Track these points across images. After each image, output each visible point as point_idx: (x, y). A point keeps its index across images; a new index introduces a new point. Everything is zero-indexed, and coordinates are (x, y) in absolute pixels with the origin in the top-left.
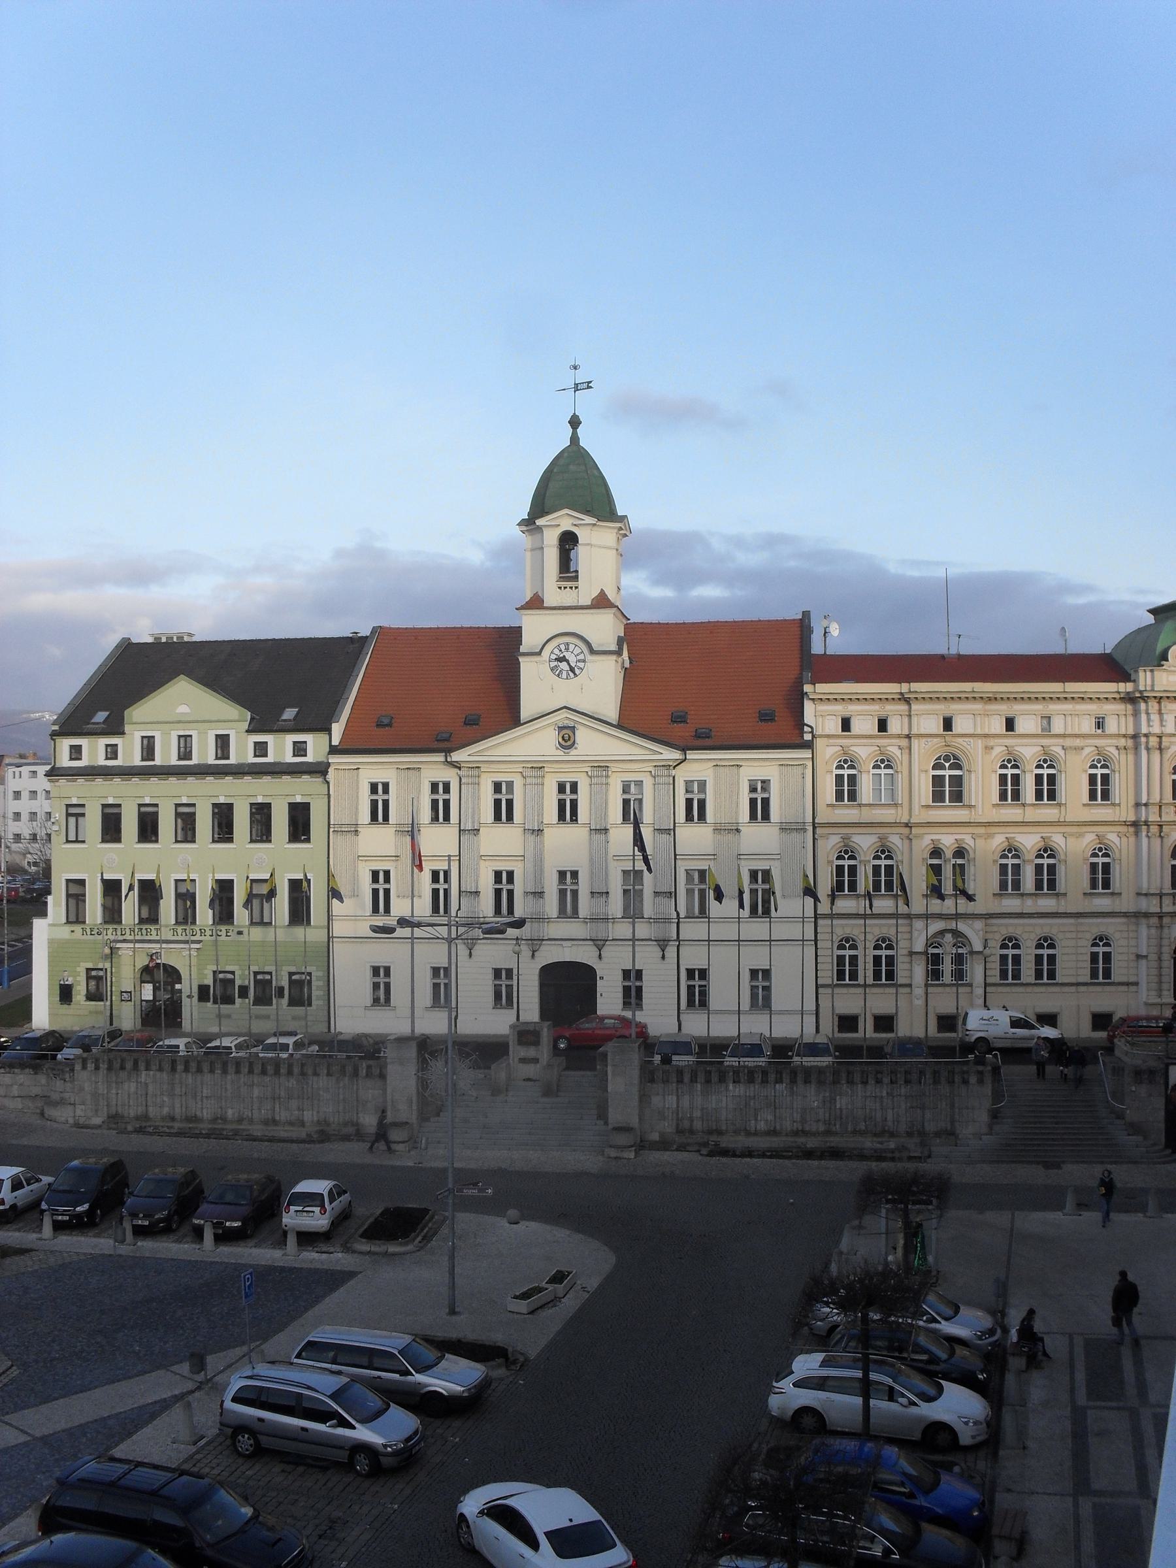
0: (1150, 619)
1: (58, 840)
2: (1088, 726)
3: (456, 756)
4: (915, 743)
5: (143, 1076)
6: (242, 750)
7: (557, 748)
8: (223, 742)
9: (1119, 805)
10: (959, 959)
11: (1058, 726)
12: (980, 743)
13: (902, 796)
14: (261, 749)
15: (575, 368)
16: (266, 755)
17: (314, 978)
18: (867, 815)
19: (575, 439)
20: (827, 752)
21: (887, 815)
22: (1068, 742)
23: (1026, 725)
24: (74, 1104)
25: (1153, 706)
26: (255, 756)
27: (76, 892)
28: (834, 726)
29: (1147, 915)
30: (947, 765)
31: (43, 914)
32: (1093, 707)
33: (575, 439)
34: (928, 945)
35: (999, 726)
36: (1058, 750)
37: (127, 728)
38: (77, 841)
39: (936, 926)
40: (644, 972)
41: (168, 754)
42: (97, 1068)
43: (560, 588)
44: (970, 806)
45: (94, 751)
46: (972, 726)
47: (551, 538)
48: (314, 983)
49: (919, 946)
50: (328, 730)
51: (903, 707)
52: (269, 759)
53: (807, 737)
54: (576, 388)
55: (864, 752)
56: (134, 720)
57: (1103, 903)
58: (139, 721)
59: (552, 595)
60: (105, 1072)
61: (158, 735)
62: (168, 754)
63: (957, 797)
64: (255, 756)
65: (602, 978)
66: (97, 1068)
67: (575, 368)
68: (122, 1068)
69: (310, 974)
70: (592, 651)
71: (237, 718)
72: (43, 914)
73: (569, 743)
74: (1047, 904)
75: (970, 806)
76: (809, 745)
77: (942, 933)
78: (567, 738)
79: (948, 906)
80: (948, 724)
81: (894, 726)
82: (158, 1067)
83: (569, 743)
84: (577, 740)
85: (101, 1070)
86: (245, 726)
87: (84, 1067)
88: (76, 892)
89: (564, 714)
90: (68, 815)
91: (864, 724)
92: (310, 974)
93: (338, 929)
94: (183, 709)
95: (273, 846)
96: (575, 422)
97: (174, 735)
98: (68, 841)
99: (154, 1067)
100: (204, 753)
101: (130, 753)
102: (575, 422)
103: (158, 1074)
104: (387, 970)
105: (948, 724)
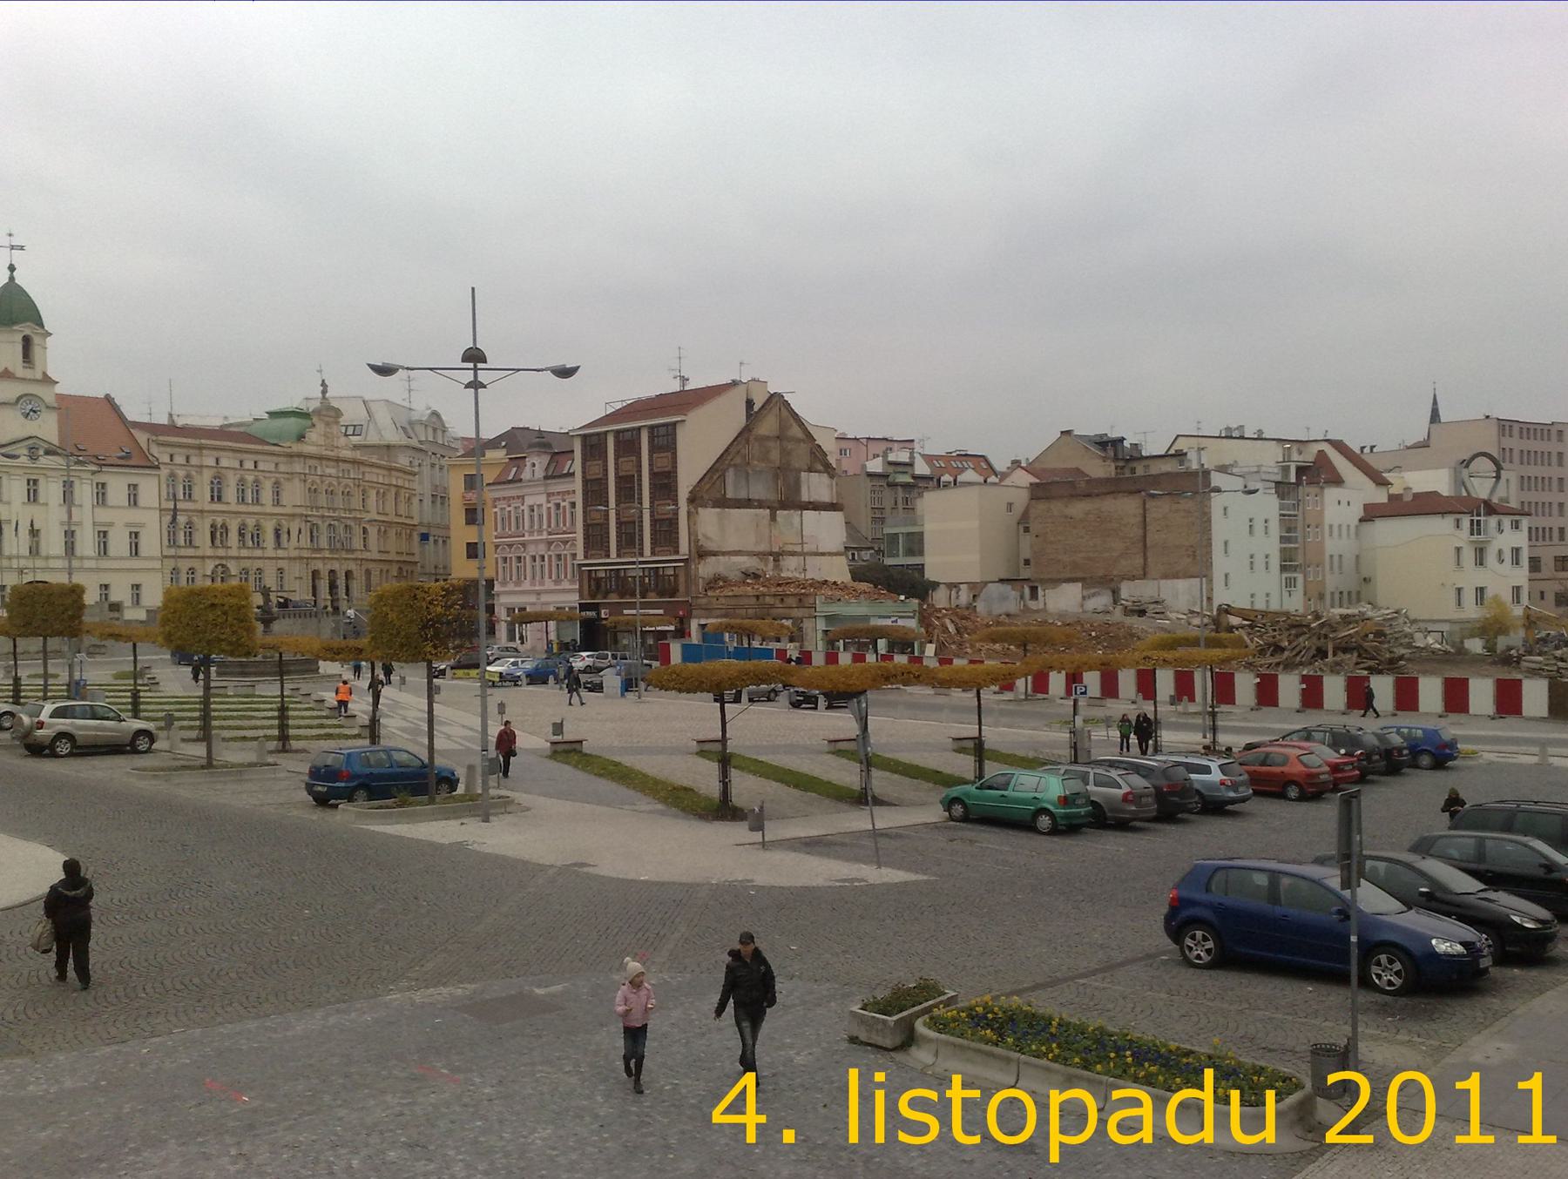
0: (266, 416)
2: (272, 467)
11: (261, 466)
12: (232, 471)
15: (10, 235)
19: (12, 279)
20: (164, 472)
22: (267, 475)
25: (302, 459)
28: (167, 460)
29: (301, 558)
32: (275, 459)
33: (12, 279)
39: (217, 563)
47: (19, 338)
51: (197, 452)
54: (12, 247)
55: (181, 473)
63: (219, 498)
67: (10, 235)
70: (48, 407)
74: (258, 553)
75: (228, 503)
76: (157, 468)
77: (216, 567)
79: (221, 552)
81: (194, 461)
89: (30, 442)
91: (180, 460)
96: (12, 268)
102: (12, 268)
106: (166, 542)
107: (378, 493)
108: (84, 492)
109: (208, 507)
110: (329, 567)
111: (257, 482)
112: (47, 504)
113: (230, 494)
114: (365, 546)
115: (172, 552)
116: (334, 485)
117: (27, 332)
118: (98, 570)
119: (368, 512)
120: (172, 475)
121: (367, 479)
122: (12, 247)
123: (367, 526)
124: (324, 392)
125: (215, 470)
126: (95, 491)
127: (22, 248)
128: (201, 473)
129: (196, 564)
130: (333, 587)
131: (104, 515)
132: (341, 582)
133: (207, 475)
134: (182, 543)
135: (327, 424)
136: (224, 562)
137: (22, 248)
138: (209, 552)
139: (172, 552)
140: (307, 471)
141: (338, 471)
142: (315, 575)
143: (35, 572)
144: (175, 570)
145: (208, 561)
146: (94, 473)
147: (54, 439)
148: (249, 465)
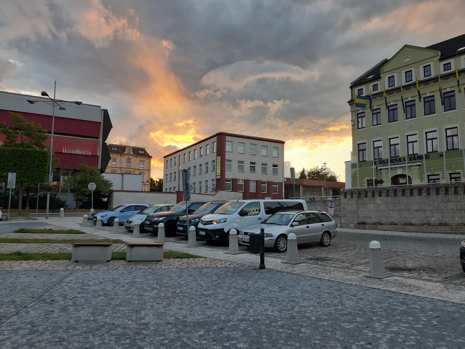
5: (378, 200)
8: (427, 68)
24: (341, 217)
37: (381, 75)
38: (362, 128)
42: (352, 197)
56: (385, 71)
58: (386, 71)
60: (356, 199)
62: (400, 81)
66: (352, 197)
68: (366, 196)
71: (433, 56)
82: (386, 194)
85: (354, 197)
86: (439, 57)
87: (346, 197)
90: (358, 118)
94: (407, 60)
95: (457, 111)
99: (383, 195)
103: (386, 198)
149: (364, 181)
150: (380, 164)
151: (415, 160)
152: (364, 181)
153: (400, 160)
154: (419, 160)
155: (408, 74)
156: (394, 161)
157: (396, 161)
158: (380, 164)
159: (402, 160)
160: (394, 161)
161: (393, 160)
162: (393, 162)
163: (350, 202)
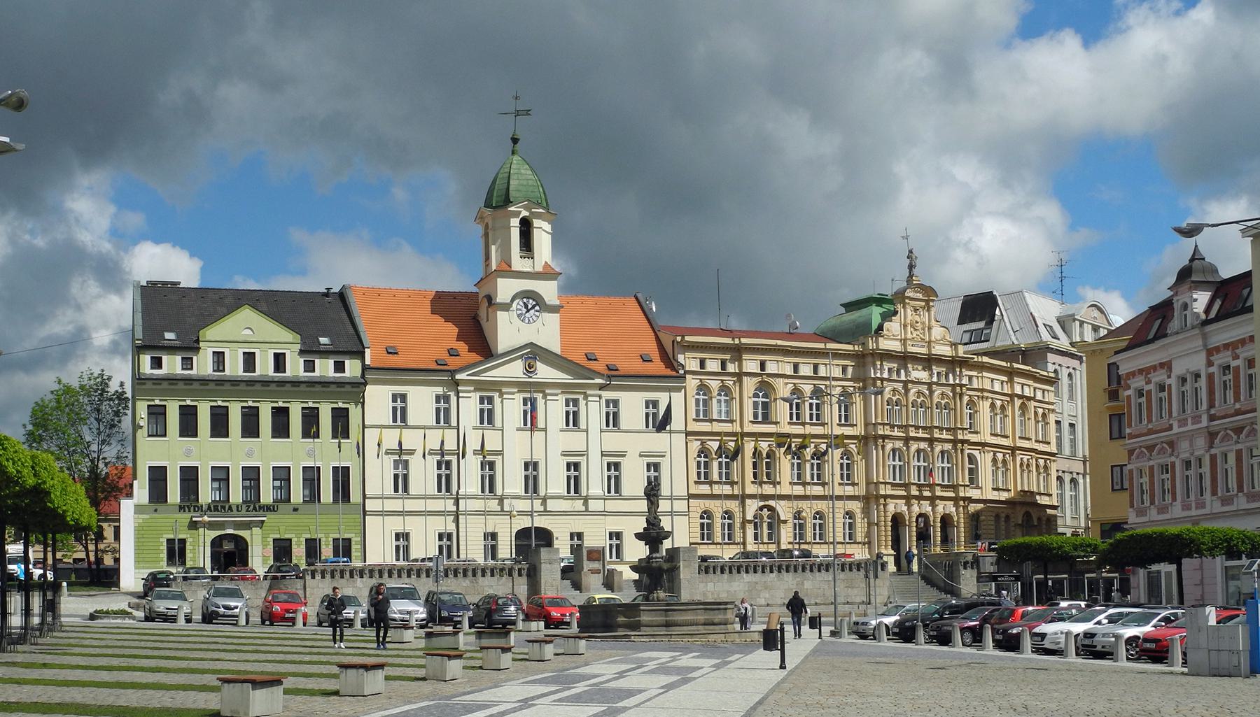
1: (142, 434)
3: (458, 377)
4: (745, 379)
6: (295, 367)
7: (524, 374)
8: (279, 361)
9: (856, 425)
10: (770, 526)
11: (822, 372)
13: (736, 416)
14: (310, 366)
16: (314, 371)
17: (353, 543)
18: (717, 427)
20: (692, 383)
21: (727, 428)
23: (806, 370)
26: (305, 371)
27: (158, 476)
28: (693, 365)
30: (761, 394)
31: (129, 495)
34: (755, 517)
35: (789, 370)
36: (823, 387)
37: (201, 344)
39: (762, 503)
40: (585, 534)
41: (234, 367)
43: (521, 257)
44: (776, 423)
45: (172, 365)
46: (776, 368)
48: (354, 547)
49: (749, 517)
50: (360, 354)
52: (317, 373)
53: (681, 372)
54: (518, 113)
55: (714, 384)
56: (207, 339)
57: (849, 491)
59: (518, 263)
61: (227, 351)
62: (234, 367)
64: (305, 371)
65: (557, 539)
69: (350, 540)
71: (291, 341)
72: (129, 495)
73: (532, 370)
74: (818, 490)
77: (761, 509)
78: (530, 369)
80: (763, 365)
81: (731, 368)
83: (532, 370)
84: (538, 369)
86: (299, 347)
88: (158, 476)
90: (149, 414)
91: (713, 366)
92: (350, 540)
93: (370, 505)
97: (241, 352)
98: (149, 436)
100: (264, 367)
101: (203, 365)
104: (408, 534)
105: (763, 365)
106: (693, 476)
107: (993, 406)
108: (593, 412)
109: (749, 428)
110: (916, 509)
111: (817, 393)
112: (545, 430)
113: (782, 411)
114: (971, 480)
115: (705, 489)
116: (924, 395)
117: (525, 213)
118: (604, 513)
119: (977, 433)
120: (703, 388)
121: (975, 386)
122: (518, 113)
123: (976, 453)
124: (911, 267)
125: (759, 379)
126: (604, 410)
127: (527, 113)
128: (740, 382)
129: (733, 505)
130: (923, 536)
131: (614, 441)
132: (936, 533)
133: (750, 384)
134: (716, 477)
135: (916, 310)
136: (772, 503)
137: (527, 112)
138: (751, 489)
139: (705, 489)
140: (886, 375)
141: (931, 375)
142: (897, 521)
143: (532, 516)
144: (707, 514)
145: (748, 501)
146: (602, 387)
147: (556, 347)
148: (806, 370)
149: (161, 540)
150: (195, 511)
151: (256, 511)
152: (161, 540)
153: (230, 508)
154: (261, 512)
155: (249, 359)
156: (219, 508)
157: (223, 511)
158: (195, 511)
159: (234, 508)
160: (219, 508)
161: (218, 506)
162: (218, 511)
163: (321, 585)
